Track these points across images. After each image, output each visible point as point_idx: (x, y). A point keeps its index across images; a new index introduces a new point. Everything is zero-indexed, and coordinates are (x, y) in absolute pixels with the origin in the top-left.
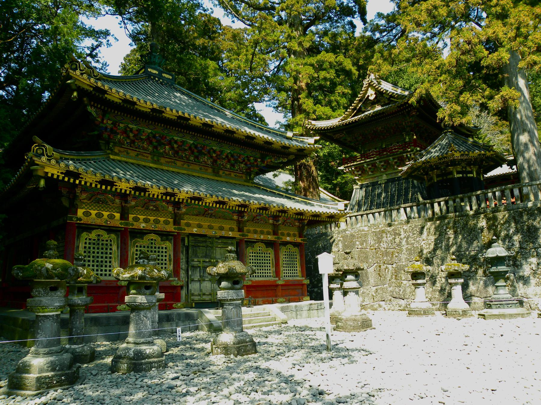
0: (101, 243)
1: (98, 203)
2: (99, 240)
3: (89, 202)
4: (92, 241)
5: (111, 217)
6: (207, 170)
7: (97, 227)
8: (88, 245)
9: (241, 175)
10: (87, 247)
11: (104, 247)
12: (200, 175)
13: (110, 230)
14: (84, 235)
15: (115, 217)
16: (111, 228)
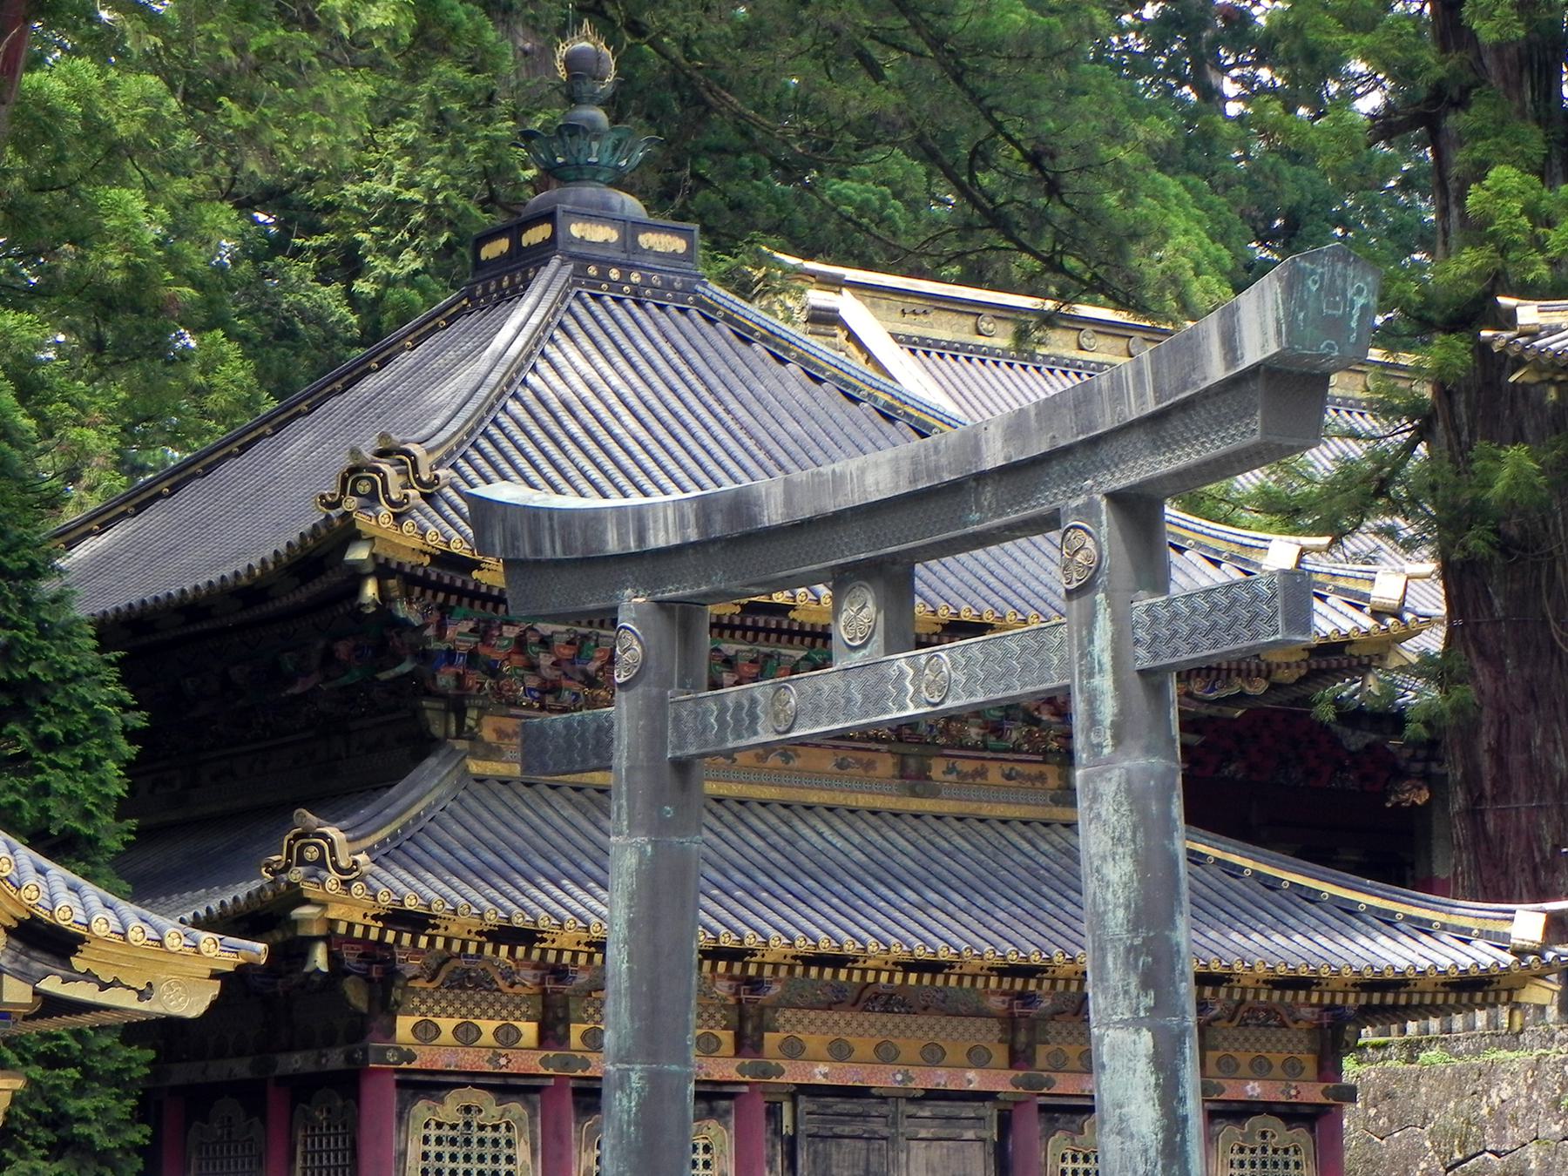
0: (476, 1135)
1: (462, 987)
2: (468, 1125)
3: (431, 986)
4: (446, 1132)
5: (508, 1037)
6: (869, 766)
7: (462, 1079)
8: (433, 1148)
9: (1033, 769)
10: (432, 1155)
11: (489, 1150)
12: (838, 798)
13: (506, 1087)
14: (421, 1110)
15: (519, 1035)
16: (512, 1081)
